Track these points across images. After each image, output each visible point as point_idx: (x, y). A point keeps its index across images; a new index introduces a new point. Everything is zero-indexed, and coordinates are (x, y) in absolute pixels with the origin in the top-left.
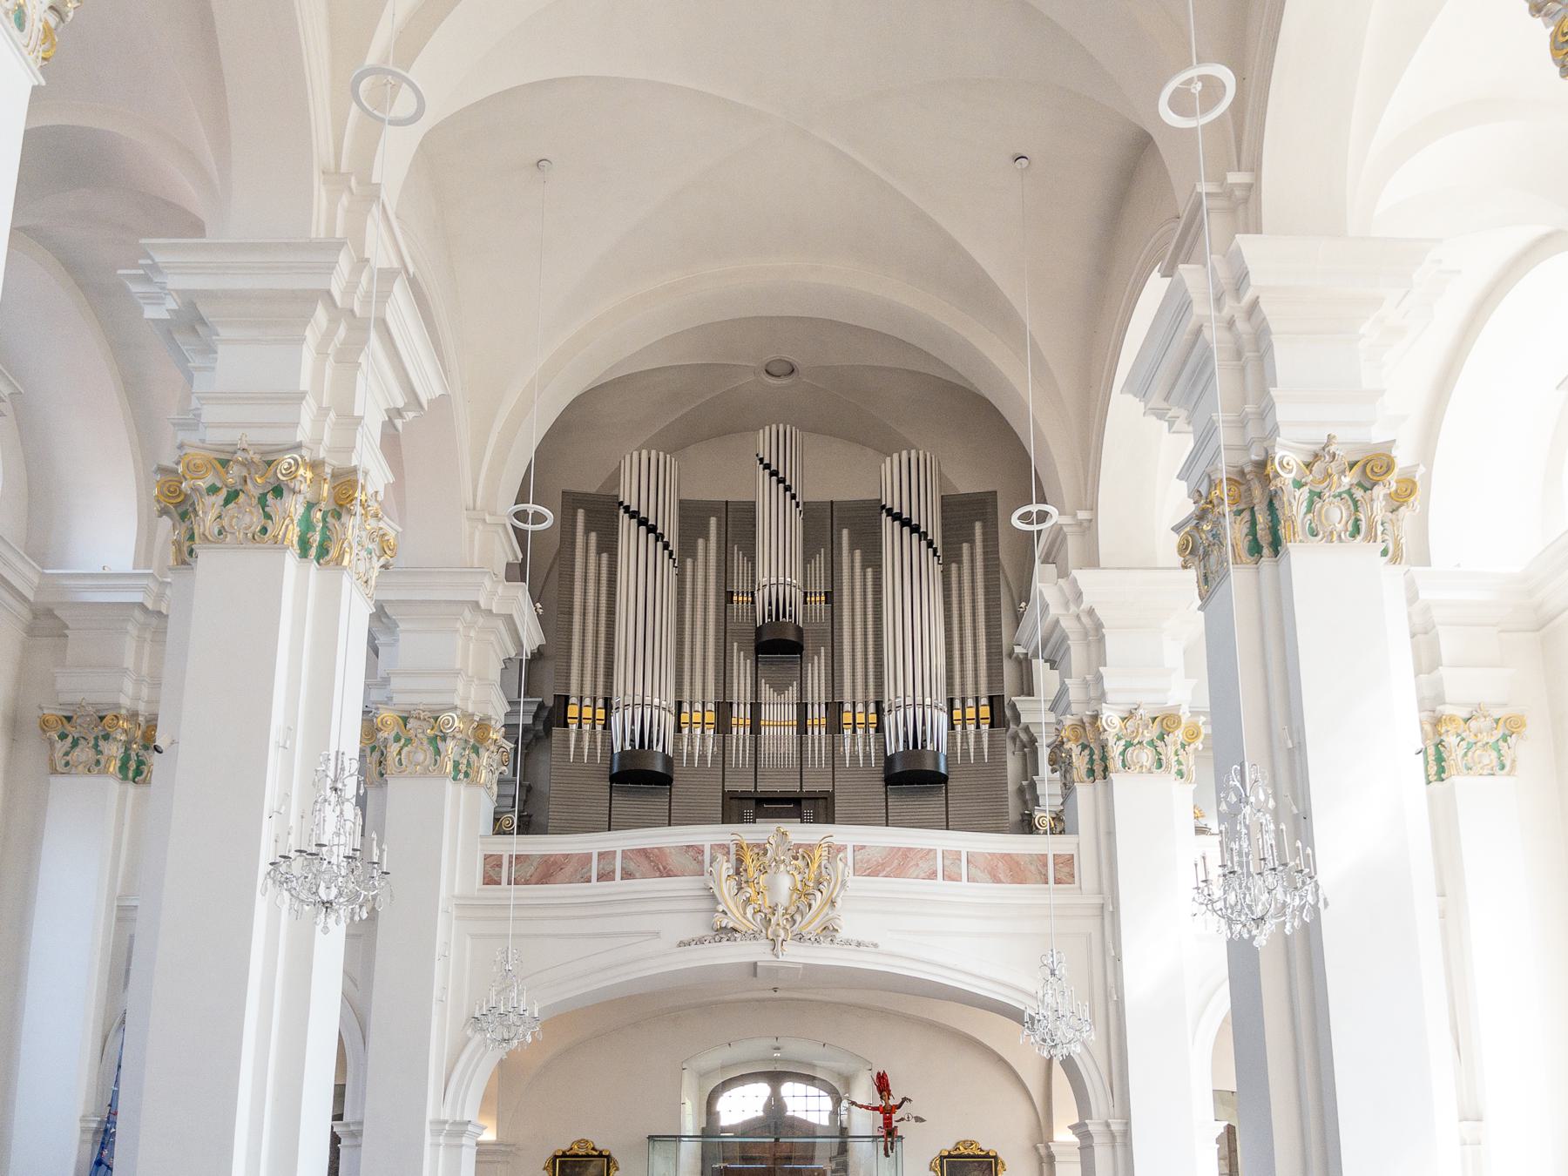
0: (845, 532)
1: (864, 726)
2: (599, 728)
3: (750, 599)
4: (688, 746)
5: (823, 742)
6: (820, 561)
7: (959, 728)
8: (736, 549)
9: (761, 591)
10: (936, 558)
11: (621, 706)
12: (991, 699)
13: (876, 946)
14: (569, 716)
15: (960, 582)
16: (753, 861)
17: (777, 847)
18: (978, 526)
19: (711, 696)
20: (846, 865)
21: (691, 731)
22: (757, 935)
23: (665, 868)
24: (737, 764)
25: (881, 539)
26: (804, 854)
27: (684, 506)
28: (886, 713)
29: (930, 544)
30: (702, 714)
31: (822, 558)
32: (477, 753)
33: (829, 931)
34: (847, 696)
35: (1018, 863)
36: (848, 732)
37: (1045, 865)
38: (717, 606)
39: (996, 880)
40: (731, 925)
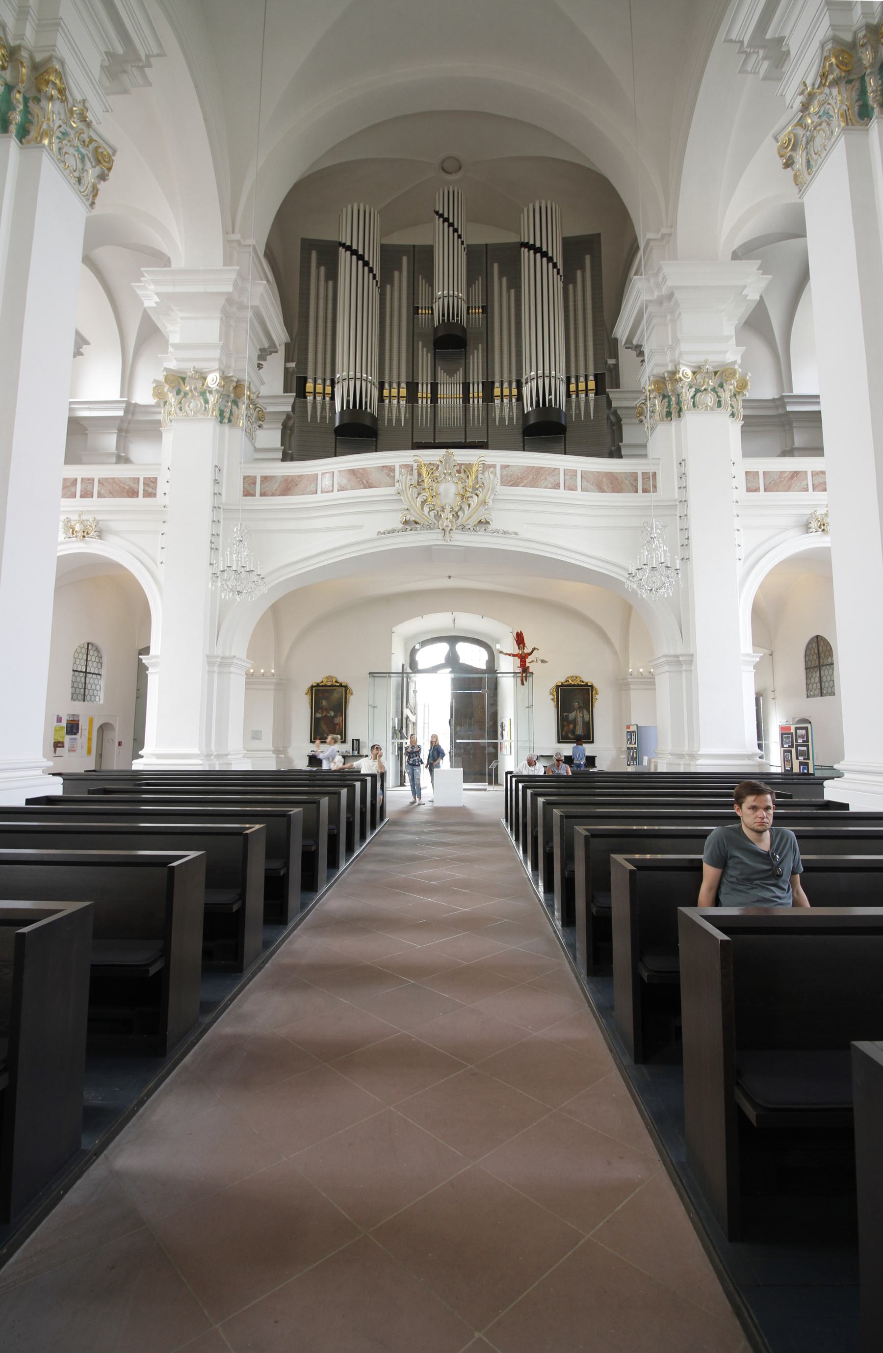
0: (496, 266)
1: (508, 397)
2: (327, 399)
3: (430, 312)
4: (389, 412)
5: (481, 408)
6: (479, 284)
7: (574, 396)
8: (420, 277)
9: (437, 303)
10: (559, 276)
11: (341, 380)
12: (596, 376)
13: (516, 534)
14: (307, 391)
15: (575, 296)
17: (446, 464)
18: (588, 258)
19: (403, 379)
21: (390, 402)
23: (367, 482)
24: (422, 424)
25: (521, 269)
26: (464, 469)
27: (384, 249)
28: (524, 385)
29: (555, 266)
30: (397, 392)
31: (480, 283)
32: (237, 406)
33: (483, 523)
34: (497, 379)
35: (616, 479)
36: (497, 401)
37: (636, 480)
38: (408, 317)
39: (601, 490)
40: (413, 519)
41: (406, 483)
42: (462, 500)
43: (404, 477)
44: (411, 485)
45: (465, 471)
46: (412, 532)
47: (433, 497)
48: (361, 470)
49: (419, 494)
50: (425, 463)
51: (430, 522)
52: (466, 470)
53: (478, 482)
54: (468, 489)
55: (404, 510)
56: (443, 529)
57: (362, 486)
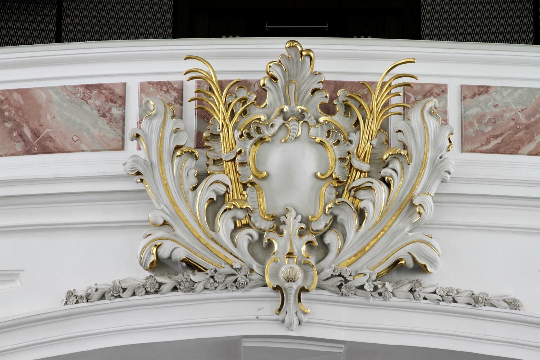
13: (514, 304)
16: (233, 114)
17: (288, 83)
20: (445, 122)
22: (242, 279)
23: (36, 134)
40: (181, 254)
41: (161, 140)
42: (339, 196)
43: (157, 122)
44: (178, 148)
45: (347, 107)
46: (178, 295)
47: (245, 186)
48: (15, 95)
49: (201, 176)
50: (221, 77)
51: (237, 265)
52: (351, 103)
53: (387, 141)
54: (356, 163)
55: (155, 225)
56: (277, 288)
57: (19, 147)
